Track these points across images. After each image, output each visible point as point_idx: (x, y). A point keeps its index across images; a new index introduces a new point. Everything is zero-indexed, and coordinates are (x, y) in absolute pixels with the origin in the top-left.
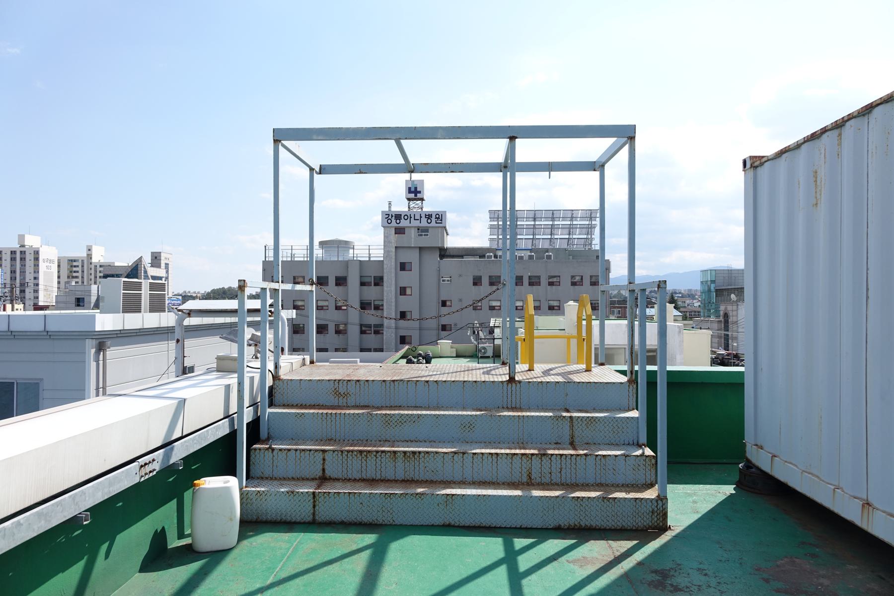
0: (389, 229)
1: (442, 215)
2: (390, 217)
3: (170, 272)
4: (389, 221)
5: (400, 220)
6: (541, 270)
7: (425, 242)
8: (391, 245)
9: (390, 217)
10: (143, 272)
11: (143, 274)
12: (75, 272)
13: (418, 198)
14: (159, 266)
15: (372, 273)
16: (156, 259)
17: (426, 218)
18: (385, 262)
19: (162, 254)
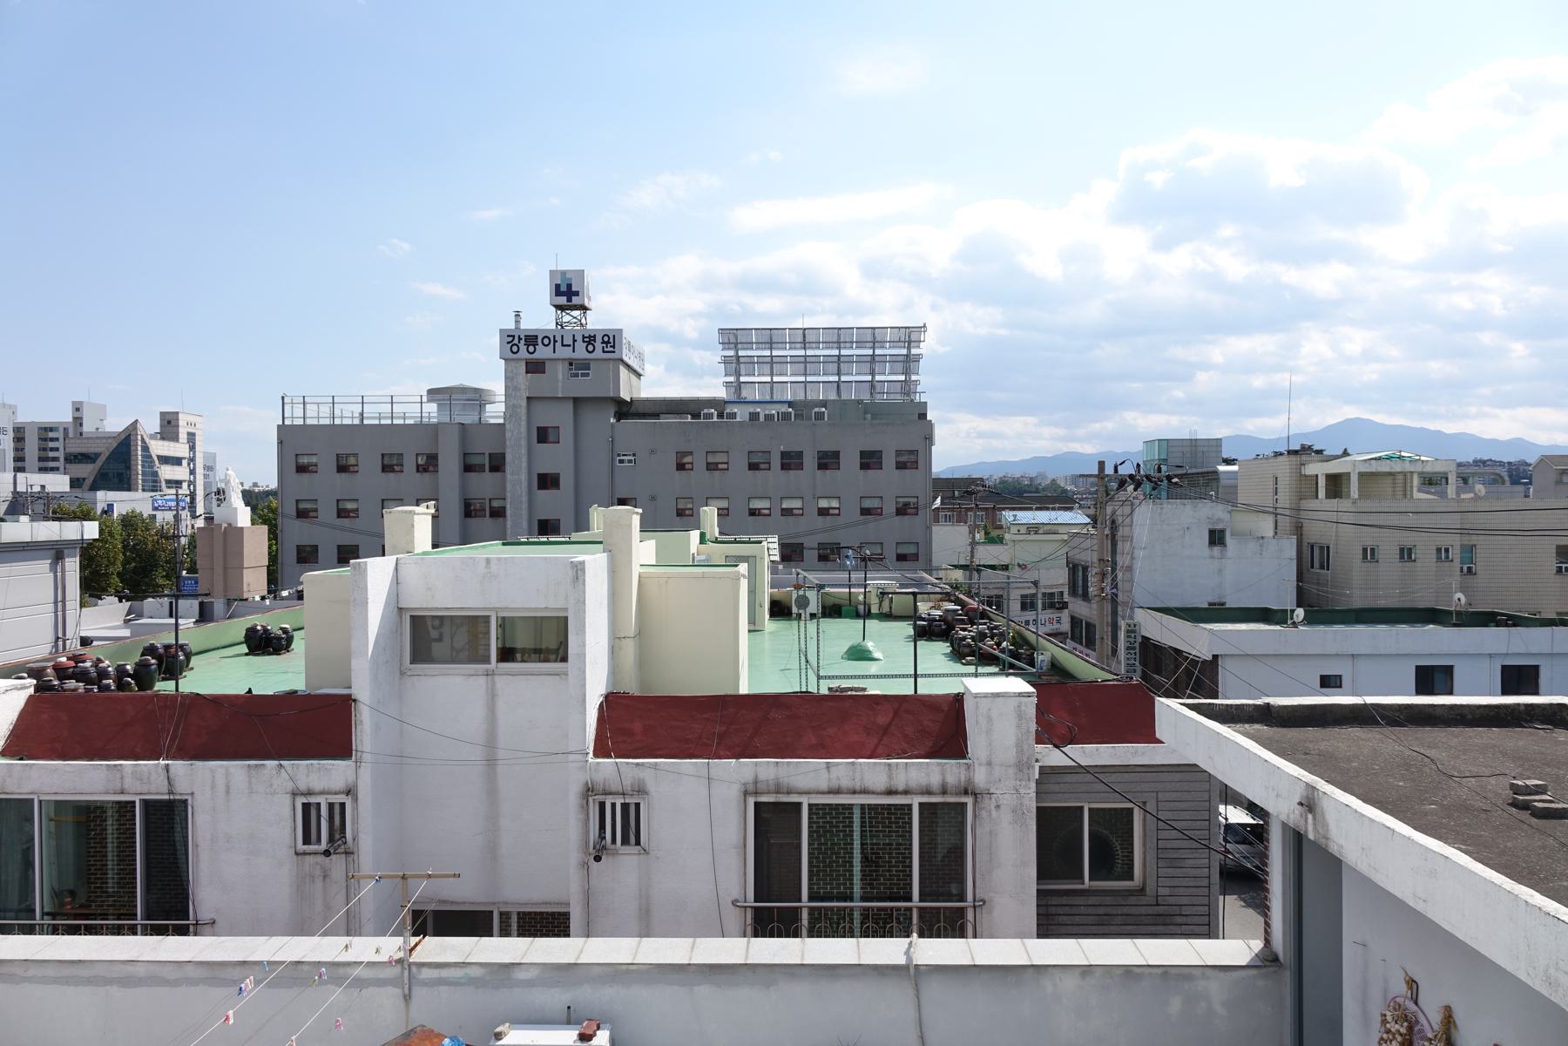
0: (513, 364)
1: (614, 336)
2: (516, 341)
3: (197, 448)
4: (515, 349)
5: (534, 346)
6: (808, 444)
7: (584, 387)
8: (518, 393)
9: (516, 341)
10: (139, 448)
11: (140, 453)
12: (52, 449)
13: (575, 306)
14: (175, 438)
15: (484, 447)
16: (169, 427)
17: (584, 341)
18: (508, 426)
19: (181, 416)
